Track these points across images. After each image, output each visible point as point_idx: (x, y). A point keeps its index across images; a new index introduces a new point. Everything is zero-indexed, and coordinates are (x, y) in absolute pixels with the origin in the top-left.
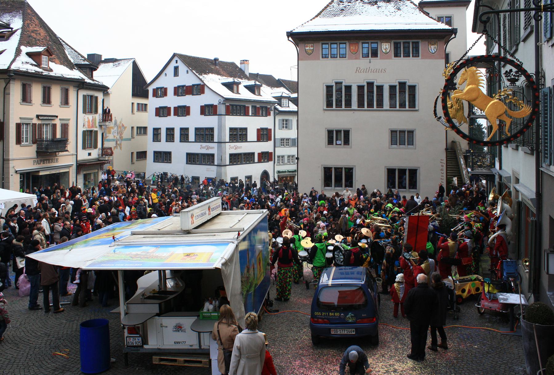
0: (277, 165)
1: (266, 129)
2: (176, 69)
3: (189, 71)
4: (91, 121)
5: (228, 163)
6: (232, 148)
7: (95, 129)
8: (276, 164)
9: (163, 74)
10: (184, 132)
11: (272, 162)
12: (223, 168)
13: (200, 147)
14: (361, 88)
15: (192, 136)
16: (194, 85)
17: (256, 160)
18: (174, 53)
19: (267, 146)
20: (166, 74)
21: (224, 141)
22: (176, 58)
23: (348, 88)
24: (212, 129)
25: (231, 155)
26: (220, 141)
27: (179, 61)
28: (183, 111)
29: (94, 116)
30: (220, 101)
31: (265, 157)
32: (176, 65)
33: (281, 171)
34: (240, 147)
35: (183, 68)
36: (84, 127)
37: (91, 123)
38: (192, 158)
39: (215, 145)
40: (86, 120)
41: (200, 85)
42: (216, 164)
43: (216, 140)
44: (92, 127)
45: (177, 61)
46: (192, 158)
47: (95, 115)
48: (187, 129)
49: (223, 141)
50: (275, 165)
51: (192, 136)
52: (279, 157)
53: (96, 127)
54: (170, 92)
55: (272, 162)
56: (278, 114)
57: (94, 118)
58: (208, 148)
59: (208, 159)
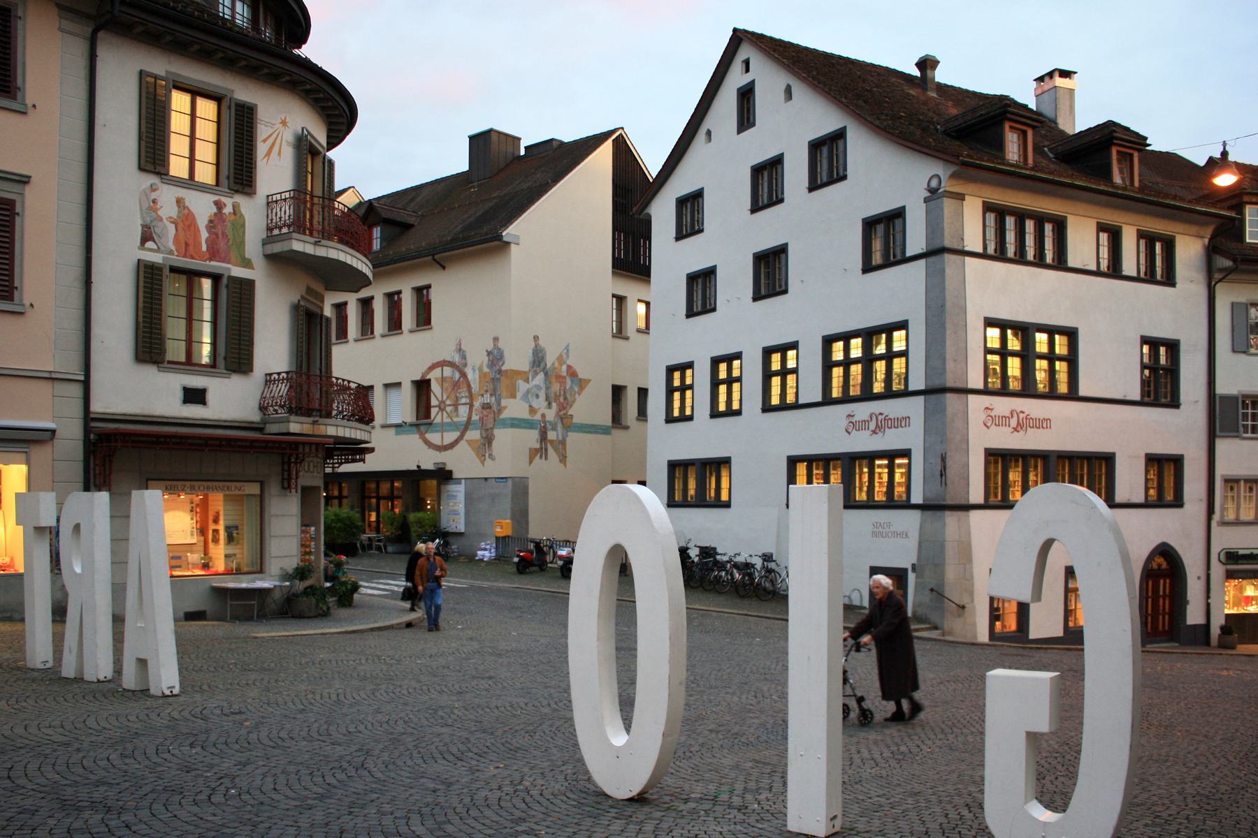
0: (1224, 523)
2: (746, 95)
3: (799, 90)
4: (202, 223)
5: (976, 494)
6: (1002, 421)
7: (238, 272)
8: (1216, 517)
9: (701, 136)
12: (951, 519)
13: (844, 423)
18: (735, 30)
20: (709, 133)
21: (959, 385)
25: (999, 459)
26: (937, 383)
29: (228, 202)
30: (934, 184)
32: (744, 80)
33: (1241, 552)
34: (1043, 423)
36: (150, 244)
37: (204, 235)
39: (914, 408)
40: (168, 210)
42: (920, 502)
44: (213, 254)
45: (747, 63)
47: (239, 199)
49: (950, 383)
50: (1214, 524)
53: (247, 264)
57: (228, 210)
58: (882, 423)
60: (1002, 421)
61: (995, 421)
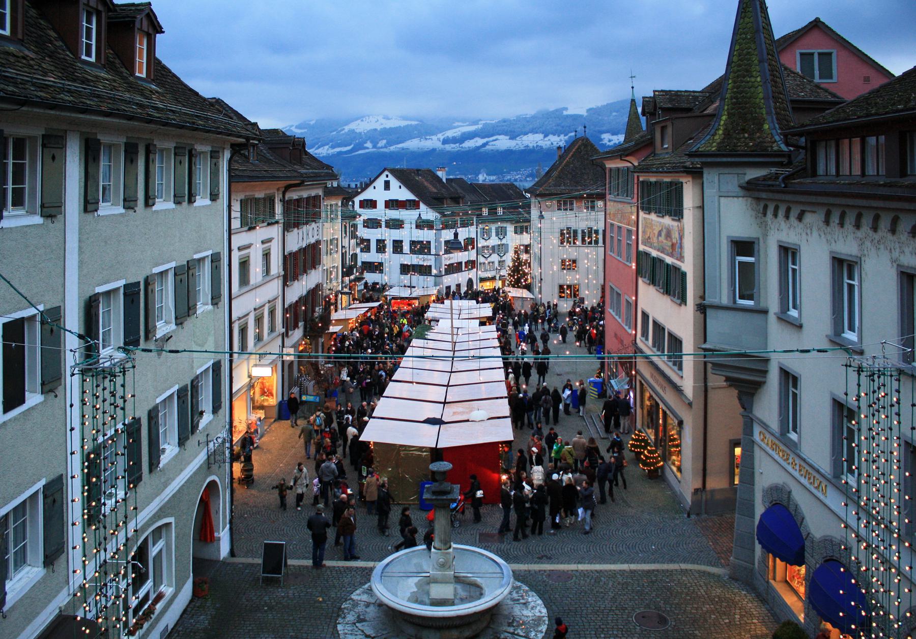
1: (471, 238)
3: (402, 186)
5: (443, 273)
10: (398, 246)
11: (475, 270)
14: (583, 232)
15: (406, 248)
16: (407, 200)
17: (463, 269)
19: (471, 255)
20: (375, 188)
22: (386, 173)
23: (575, 232)
24: (429, 242)
27: (390, 175)
28: (396, 224)
31: (471, 264)
35: (394, 183)
38: (405, 269)
39: (433, 258)
41: (414, 201)
43: (433, 251)
46: (405, 269)
48: (401, 242)
51: (406, 248)
52: (480, 264)
54: (381, 205)
55: (475, 270)
56: (481, 223)
59: (424, 270)
60: (446, 259)
61: (446, 259)
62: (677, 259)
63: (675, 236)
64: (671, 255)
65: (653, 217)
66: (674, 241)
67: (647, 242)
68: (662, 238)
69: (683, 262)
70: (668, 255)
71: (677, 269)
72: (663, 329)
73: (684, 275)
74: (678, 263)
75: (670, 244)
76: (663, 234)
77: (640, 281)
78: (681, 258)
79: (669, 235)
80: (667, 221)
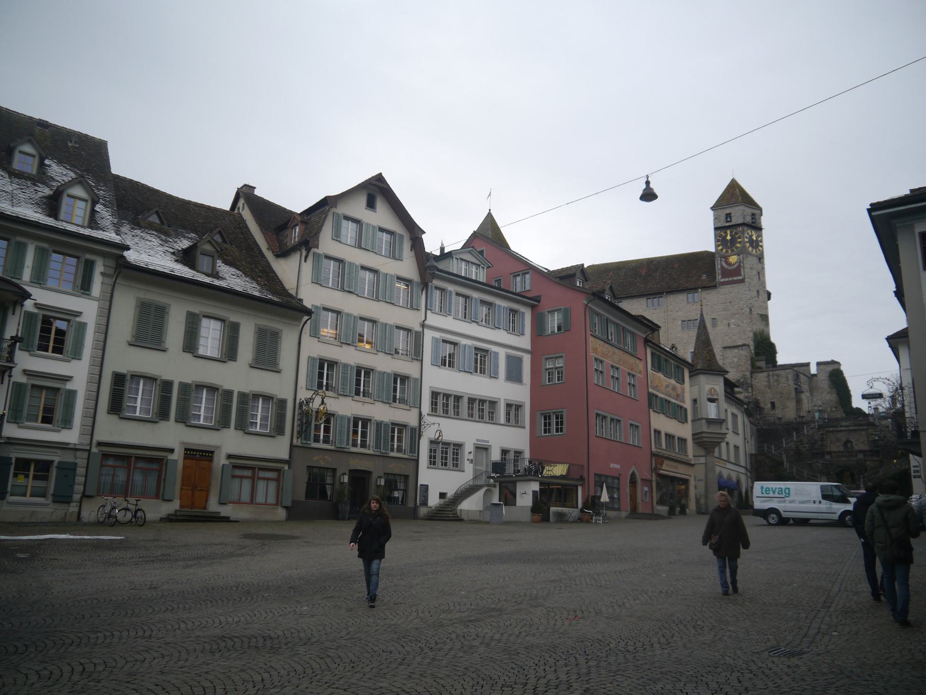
62: (680, 402)
63: (679, 391)
64: (676, 399)
65: (661, 375)
66: (679, 393)
67: (655, 388)
68: (669, 389)
69: (685, 404)
70: (673, 398)
71: (681, 407)
72: (674, 437)
73: (686, 410)
74: (681, 404)
75: (675, 394)
76: (670, 387)
77: (651, 410)
78: (683, 401)
79: (674, 388)
80: (673, 382)
